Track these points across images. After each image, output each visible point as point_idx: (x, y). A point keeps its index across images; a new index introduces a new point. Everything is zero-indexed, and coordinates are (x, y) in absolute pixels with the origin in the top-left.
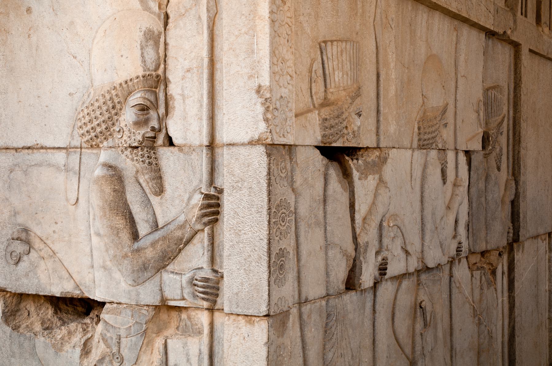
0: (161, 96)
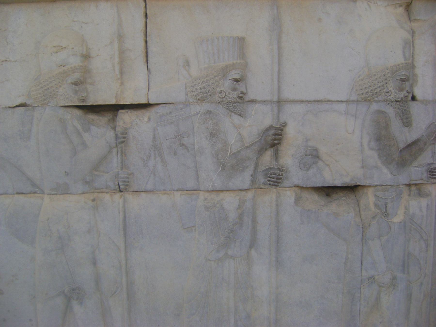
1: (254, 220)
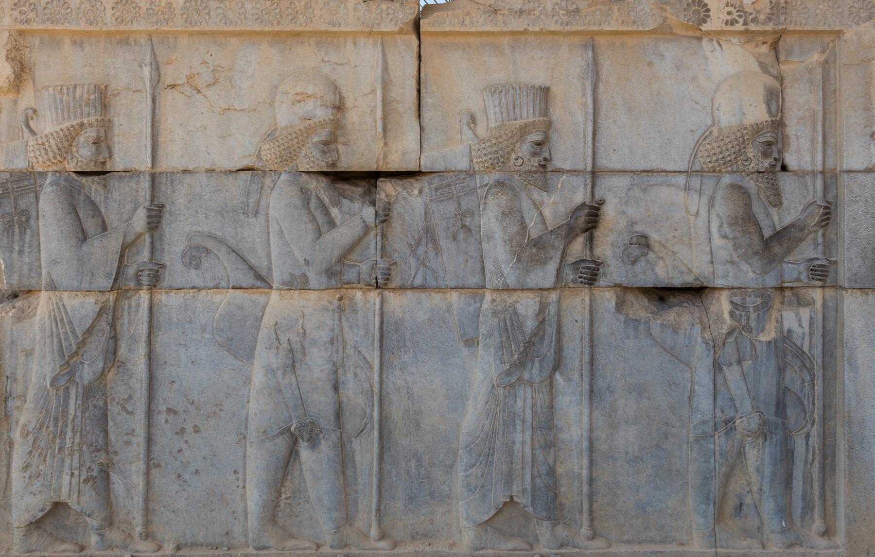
0: (779, 135)
1: (559, 331)
